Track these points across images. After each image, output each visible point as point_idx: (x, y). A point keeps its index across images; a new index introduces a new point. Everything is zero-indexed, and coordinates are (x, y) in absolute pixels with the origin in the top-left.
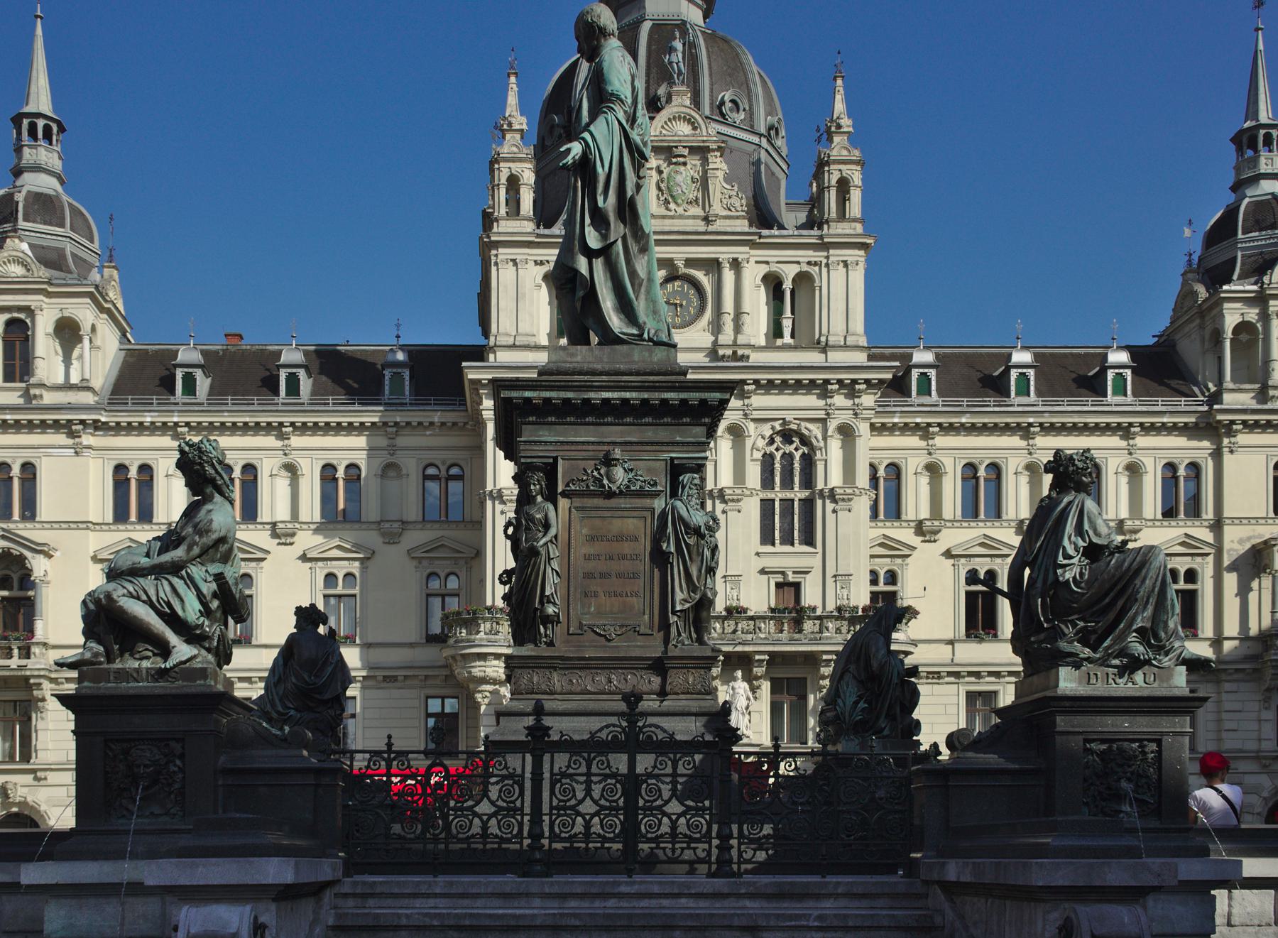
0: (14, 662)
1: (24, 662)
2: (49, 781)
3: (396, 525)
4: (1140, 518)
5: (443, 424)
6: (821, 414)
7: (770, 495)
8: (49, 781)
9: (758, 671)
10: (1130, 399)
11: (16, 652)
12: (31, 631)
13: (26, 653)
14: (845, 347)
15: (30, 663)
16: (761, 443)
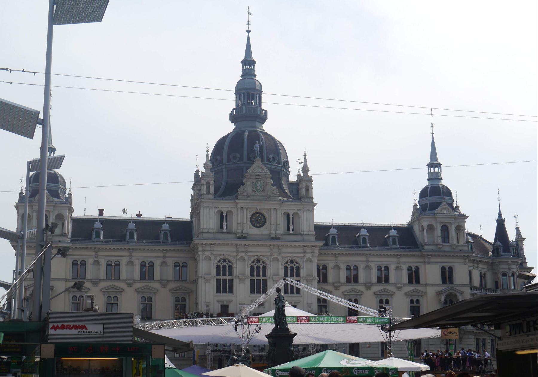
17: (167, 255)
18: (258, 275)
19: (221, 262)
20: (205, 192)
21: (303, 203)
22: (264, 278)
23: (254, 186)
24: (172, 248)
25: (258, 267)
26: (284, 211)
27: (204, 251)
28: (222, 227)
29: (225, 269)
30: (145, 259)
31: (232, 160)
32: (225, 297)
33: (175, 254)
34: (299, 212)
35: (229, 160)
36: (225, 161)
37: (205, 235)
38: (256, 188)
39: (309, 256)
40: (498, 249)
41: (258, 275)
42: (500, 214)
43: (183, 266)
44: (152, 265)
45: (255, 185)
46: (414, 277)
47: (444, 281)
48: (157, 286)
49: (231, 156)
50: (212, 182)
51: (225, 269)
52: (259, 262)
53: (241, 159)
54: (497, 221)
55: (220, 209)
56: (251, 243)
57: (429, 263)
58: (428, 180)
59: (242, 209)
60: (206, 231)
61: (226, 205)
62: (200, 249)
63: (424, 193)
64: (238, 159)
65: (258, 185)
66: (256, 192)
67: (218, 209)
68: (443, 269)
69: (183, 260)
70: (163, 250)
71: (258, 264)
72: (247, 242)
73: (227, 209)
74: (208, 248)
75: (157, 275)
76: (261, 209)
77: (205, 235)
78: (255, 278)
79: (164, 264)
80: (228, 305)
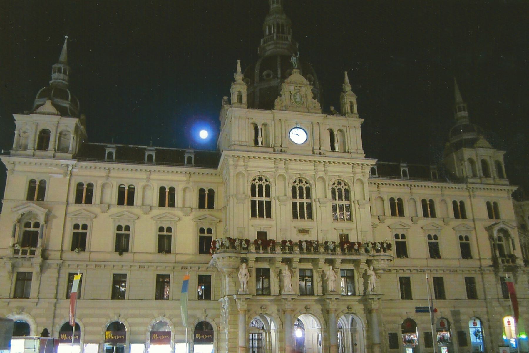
18: (301, 196)
19: (257, 180)
21: (348, 118)
22: (309, 201)
23: (292, 98)
25: (301, 189)
27: (236, 166)
28: (256, 142)
29: (260, 189)
31: (265, 77)
32: (261, 223)
34: (344, 129)
35: (261, 79)
36: (257, 79)
37: (237, 148)
38: (295, 99)
39: (359, 176)
45: (294, 96)
46: (460, 211)
47: (491, 217)
48: (179, 213)
49: (265, 73)
51: (260, 189)
52: (302, 182)
53: (275, 76)
56: (293, 157)
57: (474, 196)
60: (236, 143)
61: (261, 116)
62: (231, 162)
68: (488, 204)
72: (288, 157)
73: (263, 122)
74: (241, 163)
77: (237, 148)
78: (298, 200)
80: (265, 233)
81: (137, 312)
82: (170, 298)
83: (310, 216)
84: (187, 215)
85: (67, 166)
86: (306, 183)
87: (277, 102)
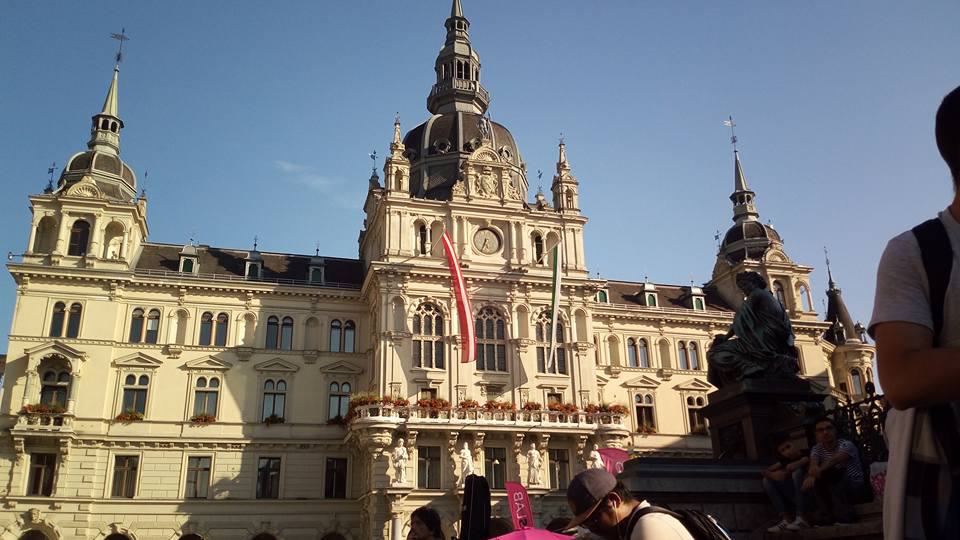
0: (51, 427)
1: (57, 428)
2: (62, 510)
3: (314, 353)
4: (619, 365)
5: (345, 297)
6: (567, 304)
7: (541, 345)
8: (62, 510)
9: (479, 443)
10: (657, 307)
11: (52, 421)
12: (65, 406)
13: (59, 422)
14: (576, 270)
15: (62, 429)
16: (536, 316)
17: (319, 306)
20: (393, 187)
24: (329, 292)
26: (532, 229)
28: (423, 251)
30: (276, 312)
33: (336, 302)
40: (840, 333)
41: (490, 336)
42: (831, 284)
43: (347, 328)
44: (289, 323)
48: (297, 359)
50: (407, 172)
54: (828, 293)
55: (421, 217)
58: (735, 219)
59: (460, 219)
61: (430, 215)
63: (734, 235)
64: (448, 147)
65: (487, 181)
66: (484, 194)
67: (415, 218)
69: (349, 316)
70: (311, 295)
71: (490, 317)
75: (299, 342)
76: (493, 222)
79: (310, 321)
81: (225, 519)
82: (280, 495)
83: (503, 368)
84: (310, 361)
85: (118, 282)
86: (498, 313)
87: (458, 187)
